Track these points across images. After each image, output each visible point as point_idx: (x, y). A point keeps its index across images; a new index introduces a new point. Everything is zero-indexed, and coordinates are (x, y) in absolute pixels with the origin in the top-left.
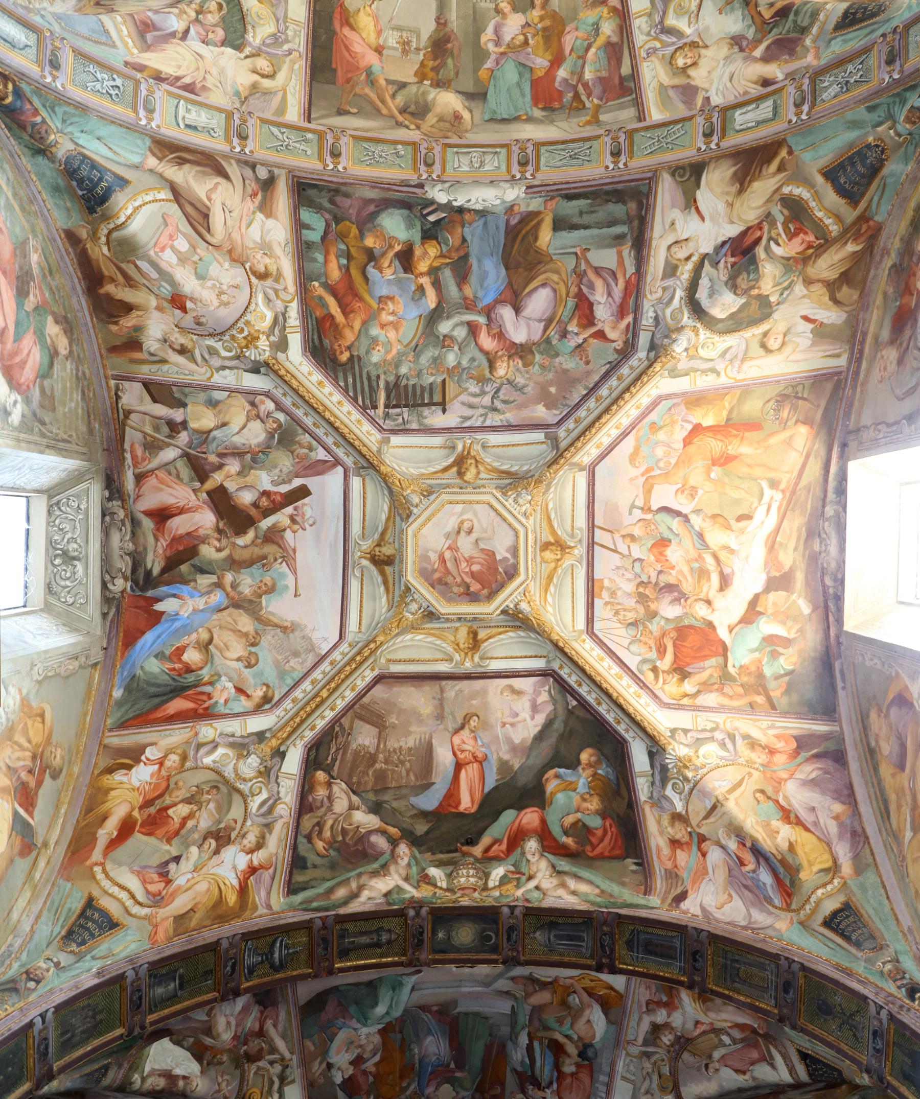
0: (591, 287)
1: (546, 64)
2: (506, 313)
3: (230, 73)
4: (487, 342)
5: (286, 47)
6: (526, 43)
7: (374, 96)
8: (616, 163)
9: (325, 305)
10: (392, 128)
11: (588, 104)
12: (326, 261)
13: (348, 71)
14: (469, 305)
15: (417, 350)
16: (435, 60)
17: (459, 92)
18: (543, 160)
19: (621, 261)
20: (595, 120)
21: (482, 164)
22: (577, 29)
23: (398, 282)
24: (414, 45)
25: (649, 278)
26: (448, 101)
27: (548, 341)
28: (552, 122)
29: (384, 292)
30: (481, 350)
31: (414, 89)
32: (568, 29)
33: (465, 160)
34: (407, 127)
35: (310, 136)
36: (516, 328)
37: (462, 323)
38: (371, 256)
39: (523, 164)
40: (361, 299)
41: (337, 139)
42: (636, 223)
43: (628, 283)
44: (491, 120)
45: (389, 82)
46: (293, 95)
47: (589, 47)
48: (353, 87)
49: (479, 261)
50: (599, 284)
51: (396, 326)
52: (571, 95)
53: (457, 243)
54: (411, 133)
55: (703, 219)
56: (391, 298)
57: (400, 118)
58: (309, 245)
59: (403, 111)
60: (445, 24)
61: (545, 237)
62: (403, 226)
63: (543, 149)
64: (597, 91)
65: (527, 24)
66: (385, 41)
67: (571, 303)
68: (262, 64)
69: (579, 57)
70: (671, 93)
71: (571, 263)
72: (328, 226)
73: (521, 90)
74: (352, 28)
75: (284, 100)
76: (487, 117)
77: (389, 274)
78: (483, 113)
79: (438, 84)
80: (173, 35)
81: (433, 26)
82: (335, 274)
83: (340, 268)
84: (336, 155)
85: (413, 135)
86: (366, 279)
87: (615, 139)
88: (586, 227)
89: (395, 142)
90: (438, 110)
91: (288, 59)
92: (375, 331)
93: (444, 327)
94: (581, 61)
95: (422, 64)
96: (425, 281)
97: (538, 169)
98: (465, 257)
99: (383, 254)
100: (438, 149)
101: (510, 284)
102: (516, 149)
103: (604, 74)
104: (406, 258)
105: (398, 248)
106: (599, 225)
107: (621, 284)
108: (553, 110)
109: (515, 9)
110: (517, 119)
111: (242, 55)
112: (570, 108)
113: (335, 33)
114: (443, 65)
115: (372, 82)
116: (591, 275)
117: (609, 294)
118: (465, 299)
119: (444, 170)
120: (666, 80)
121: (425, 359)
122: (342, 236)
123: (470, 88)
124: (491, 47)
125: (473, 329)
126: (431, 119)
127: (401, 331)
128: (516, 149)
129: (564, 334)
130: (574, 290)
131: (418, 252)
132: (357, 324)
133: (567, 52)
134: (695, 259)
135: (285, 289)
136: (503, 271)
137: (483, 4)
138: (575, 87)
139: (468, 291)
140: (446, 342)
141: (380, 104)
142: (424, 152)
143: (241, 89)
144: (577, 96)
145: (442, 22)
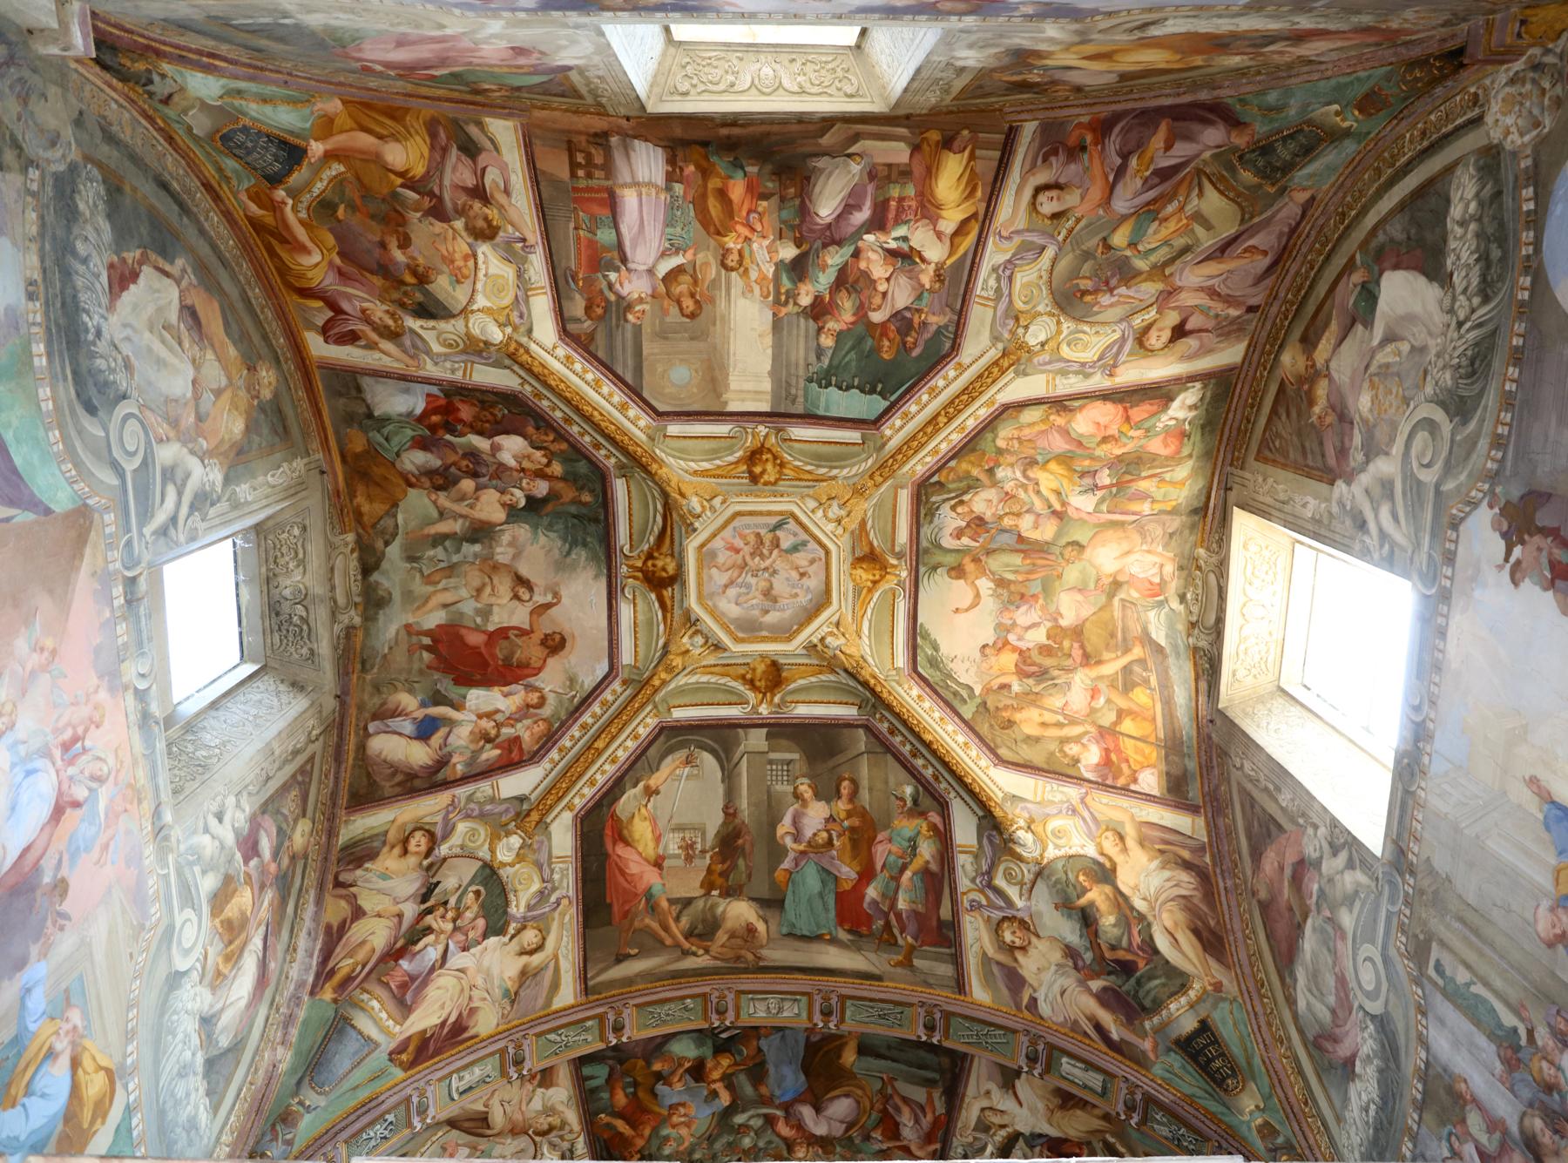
0: (898, 1110)
1: (854, 876)
2: (807, 1112)
3: (495, 972)
4: (784, 1130)
5: (553, 899)
6: (830, 843)
7: (655, 925)
8: (930, 1037)
9: (614, 1128)
10: (678, 960)
11: (900, 942)
12: (612, 1095)
13: (625, 902)
14: (766, 1101)
15: (711, 1139)
16: (723, 862)
17: (753, 899)
18: (848, 1013)
19: (930, 1099)
20: (907, 963)
21: (780, 1010)
22: (890, 841)
23: (688, 1090)
24: (699, 846)
25: (959, 1125)
26: (740, 911)
27: (850, 1139)
28: (859, 949)
29: (675, 1100)
30: (779, 1135)
31: (700, 904)
32: (880, 837)
33: (761, 1006)
34: (695, 954)
35: (589, 1023)
36: (816, 1124)
37: (758, 1115)
38: (659, 1076)
39: (827, 1014)
40: (649, 1112)
41: (619, 1014)
42: (949, 1076)
43: (936, 1120)
44: (790, 935)
45: (671, 901)
46: (566, 957)
47: (904, 868)
48: (632, 920)
49: (776, 1066)
50: (906, 1111)
51: (688, 1125)
52: (881, 922)
53: (753, 1052)
54: (699, 960)
55: (1021, 1104)
56: (683, 1105)
57: (686, 945)
58: (594, 1091)
59: (689, 935)
60: (734, 815)
61: (849, 1057)
62: (692, 1046)
63: (849, 1003)
64: (912, 927)
65: (831, 819)
66: (665, 848)
67: (875, 1115)
68: (530, 937)
69: (892, 878)
70: (995, 969)
71: (879, 1085)
72: (612, 1069)
73: (825, 904)
74: (627, 844)
75: (557, 970)
76: (785, 930)
77: (679, 1087)
78: (780, 925)
79: (728, 893)
80: (432, 969)
81: (719, 818)
82: (621, 1099)
83: (626, 1096)
84: (618, 1029)
85: (702, 961)
86: (655, 1096)
87: (929, 1013)
88: (894, 1060)
89: (683, 998)
90: (729, 924)
91: (556, 915)
92: (665, 1132)
93: (739, 1119)
94: (893, 884)
95: (709, 871)
96: (718, 1086)
97: (842, 1020)
98: (762, 1064)
99: (673, 1073)
100: (730, 997)
101: (810, 1089)
102: (818, 1000)
103: (920, 908)
104: (698, 1071)
105: (687, 1065)
106: (909, 1064)
107: (930, 1117)
108: (861, 936)
109: (818, 796)
110: (818, 938)
111: (506, 939)
112: (880, 939)
113: (607, 856)
114: (734, 867)
115: (653, 908)
116: (900, 1103)
117: (917, 1121)
118: (761, 1096)
119: (738, 1015)
120: (991, 952)
121: (718, 1146)
122: (626, 1073)
123: (765, 892)
124: (788, 841)
125: (770, 1121)
126: (721, 937)
127: (694, 1127)
128: (818, 1000)
129: (867, 1138)
130: (878, 1106)
131: (709, 1064)
132: (647, 1132)
133: (879, 866)
134: (1010, 1130)
135: (571, 1131)
136: (803, 1078)
137: (779, 787)
138: (886, 915)
139: (764, 1090)
140: (743, 1129)
141: (663, 933)
142: (715, 1001)
143: (509, 984)
144: (888, 926)
145: (730, 812)
